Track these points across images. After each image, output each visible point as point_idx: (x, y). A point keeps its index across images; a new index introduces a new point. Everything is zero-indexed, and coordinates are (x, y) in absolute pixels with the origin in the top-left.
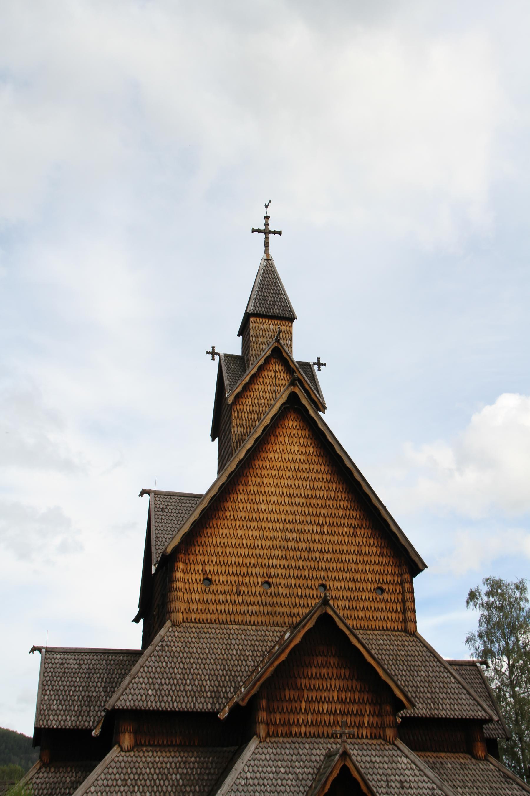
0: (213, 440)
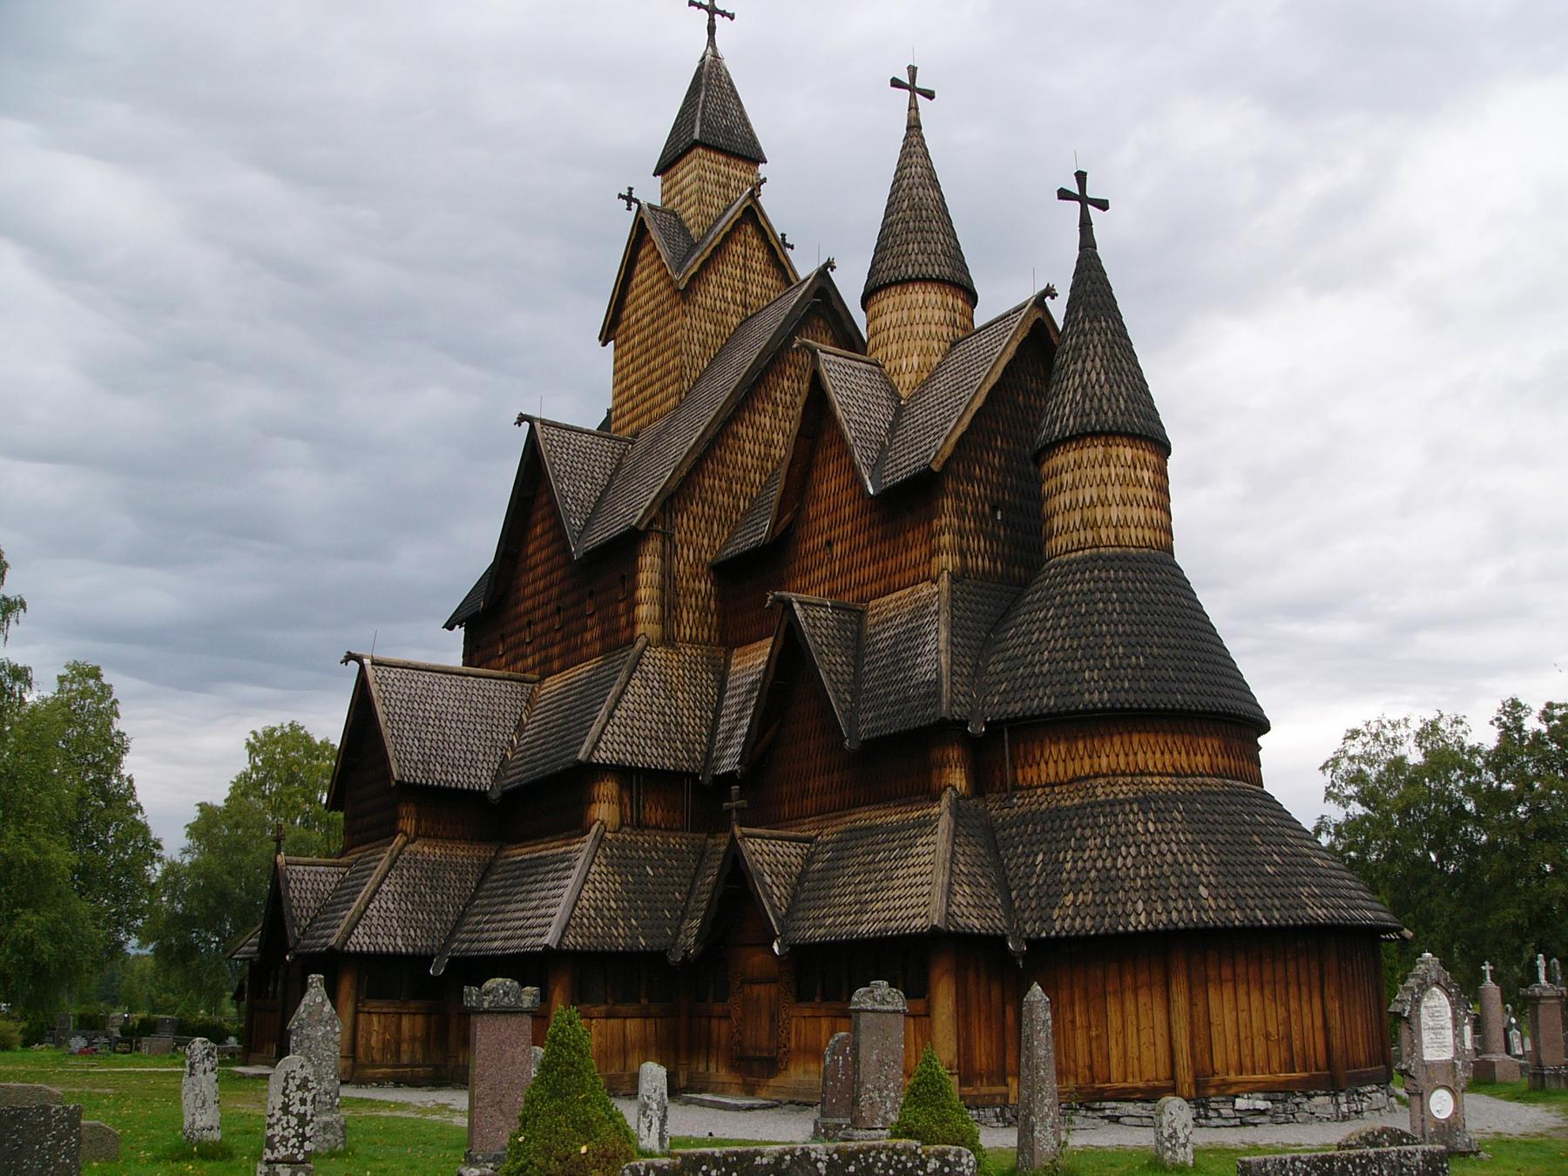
0: (604, 344)
